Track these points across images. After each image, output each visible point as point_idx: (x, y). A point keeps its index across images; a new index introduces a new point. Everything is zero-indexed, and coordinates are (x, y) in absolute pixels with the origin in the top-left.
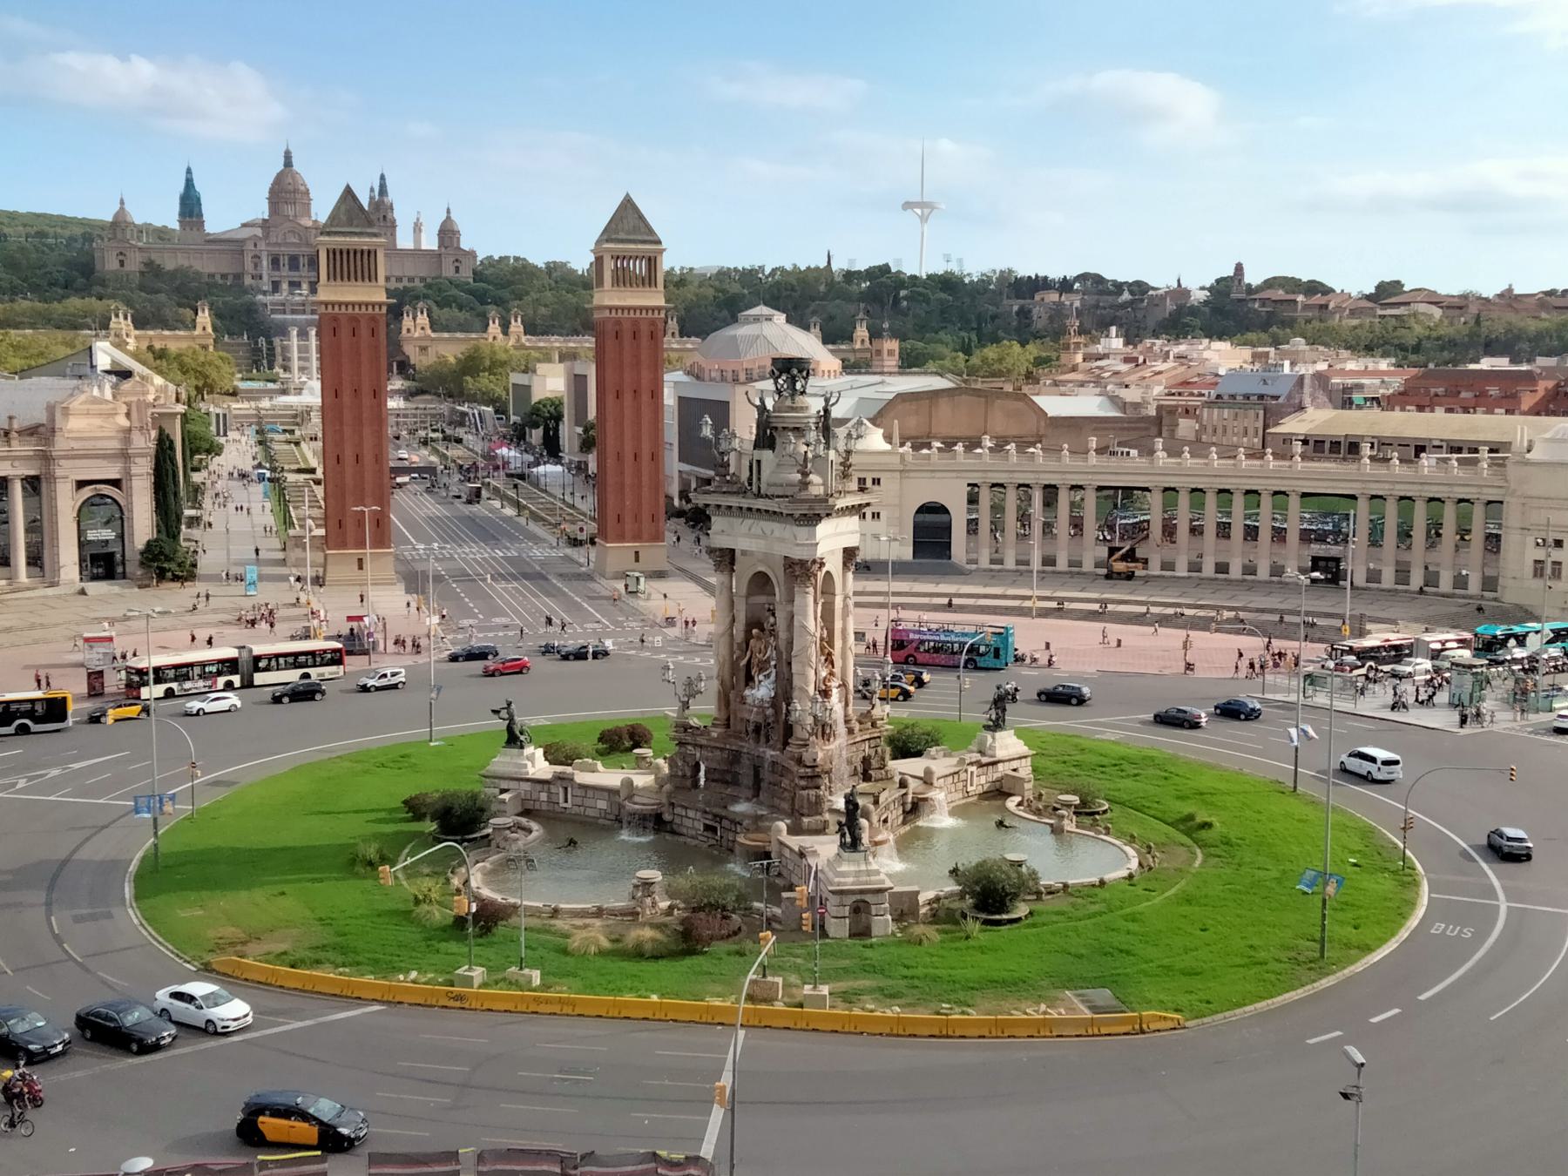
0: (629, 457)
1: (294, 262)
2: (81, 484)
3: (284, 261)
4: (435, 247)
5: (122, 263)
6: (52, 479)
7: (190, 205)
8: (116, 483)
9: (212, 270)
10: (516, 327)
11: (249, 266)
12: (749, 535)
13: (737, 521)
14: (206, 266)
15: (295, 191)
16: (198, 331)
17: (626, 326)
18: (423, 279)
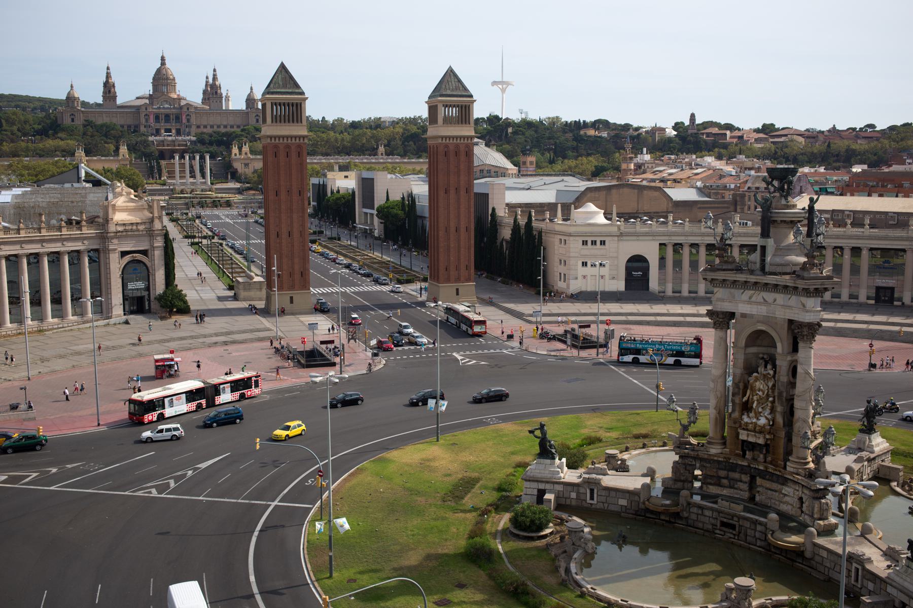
0: (453, 230)
1: (167, 117)
2: (124, 254)
3: (162, 117)
4: (244, 108)
5: (73, 120)
6: (107, 251)
7: (109, 89)
8: (144, 253)
9: (122, 123)
11: (143, 120)
12: (749, 302)
13: (737, 292)
14: (118, 121)
16: (121, 157)
17: (451, 148)
18: (238, 127)
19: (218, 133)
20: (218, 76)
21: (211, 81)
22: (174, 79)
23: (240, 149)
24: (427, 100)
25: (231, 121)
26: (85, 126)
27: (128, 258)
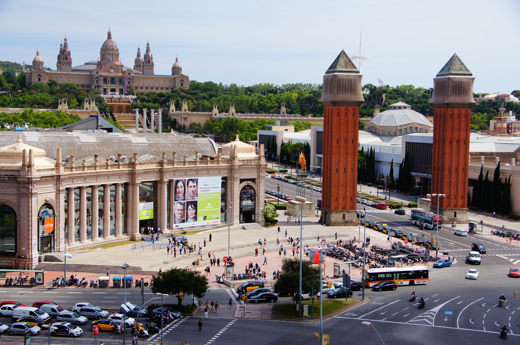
2: (242, 181)
3: (109, 80)
4: (170, 74)
5: (39, 80)
6: (232, 178)
8: (253, 180)
9: (78, 83)
10: (232, 110)
15: (113, 50)
18: (167, 89)
19: (155, 93)
20: (151, 49)
21: (143, 53)
22: (118, 50)
23: (178, 107)
24: (435, 77)
25: (161, 84)
26: (50, 85)
27: (244, 184)
